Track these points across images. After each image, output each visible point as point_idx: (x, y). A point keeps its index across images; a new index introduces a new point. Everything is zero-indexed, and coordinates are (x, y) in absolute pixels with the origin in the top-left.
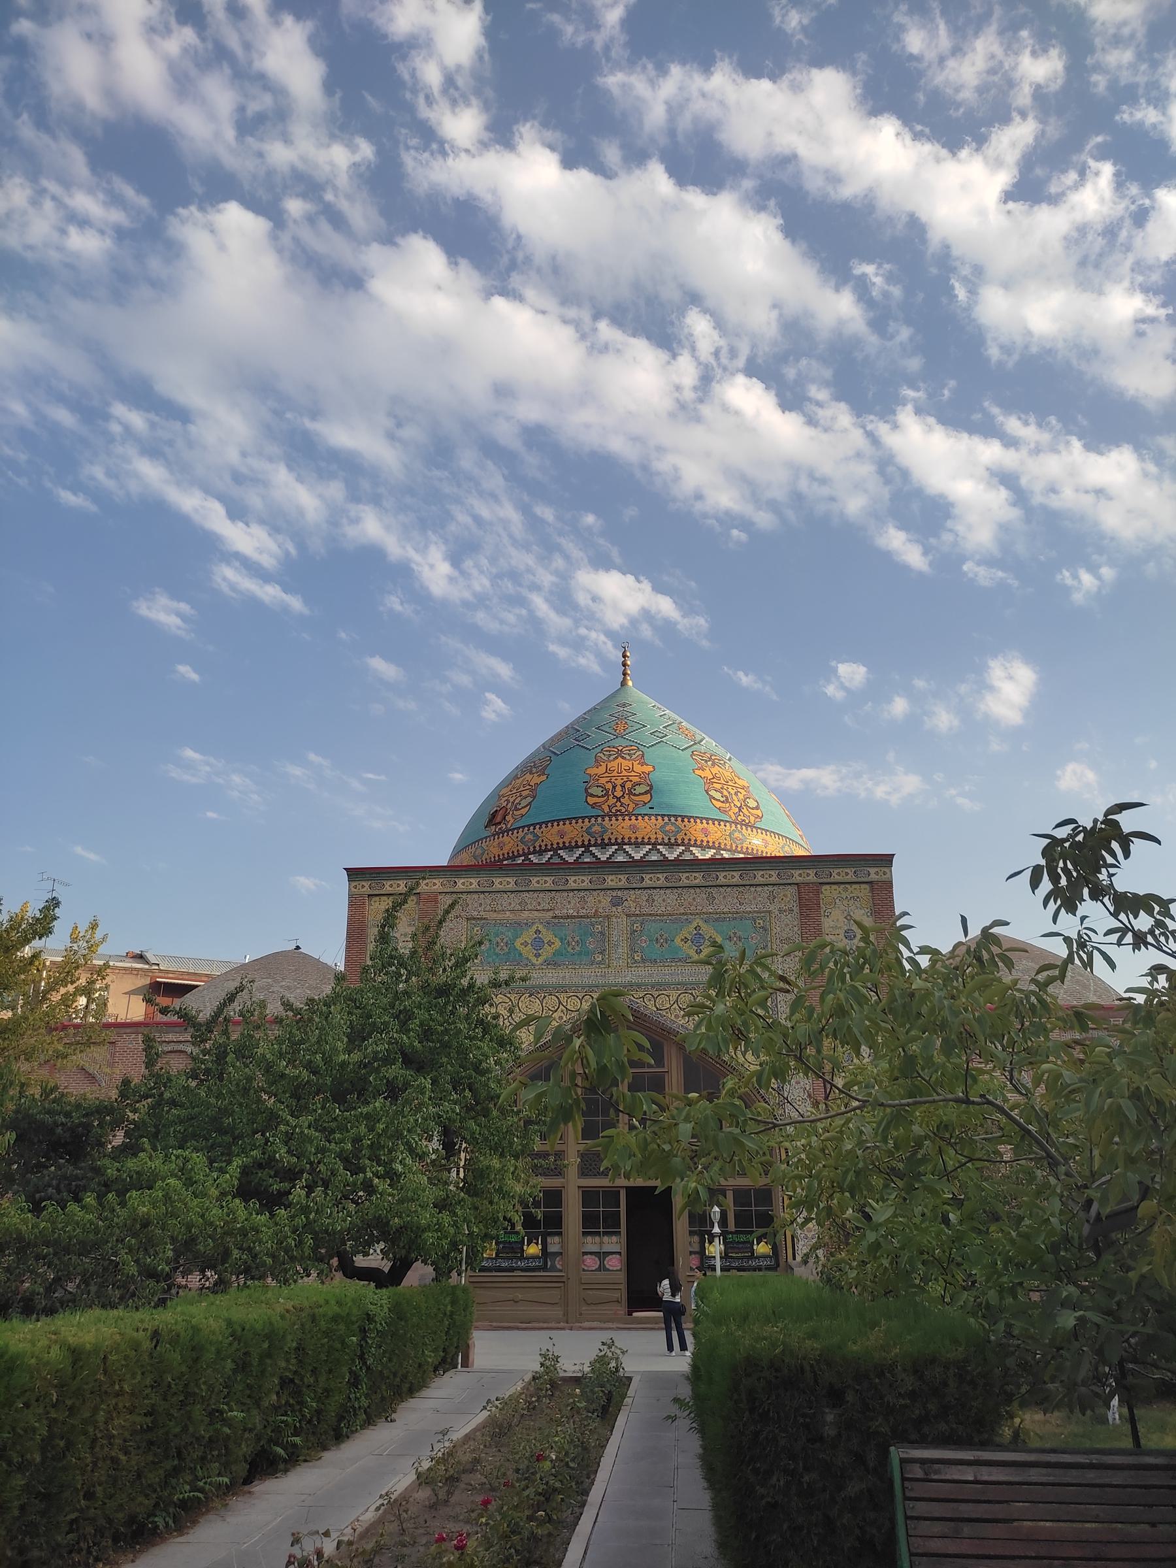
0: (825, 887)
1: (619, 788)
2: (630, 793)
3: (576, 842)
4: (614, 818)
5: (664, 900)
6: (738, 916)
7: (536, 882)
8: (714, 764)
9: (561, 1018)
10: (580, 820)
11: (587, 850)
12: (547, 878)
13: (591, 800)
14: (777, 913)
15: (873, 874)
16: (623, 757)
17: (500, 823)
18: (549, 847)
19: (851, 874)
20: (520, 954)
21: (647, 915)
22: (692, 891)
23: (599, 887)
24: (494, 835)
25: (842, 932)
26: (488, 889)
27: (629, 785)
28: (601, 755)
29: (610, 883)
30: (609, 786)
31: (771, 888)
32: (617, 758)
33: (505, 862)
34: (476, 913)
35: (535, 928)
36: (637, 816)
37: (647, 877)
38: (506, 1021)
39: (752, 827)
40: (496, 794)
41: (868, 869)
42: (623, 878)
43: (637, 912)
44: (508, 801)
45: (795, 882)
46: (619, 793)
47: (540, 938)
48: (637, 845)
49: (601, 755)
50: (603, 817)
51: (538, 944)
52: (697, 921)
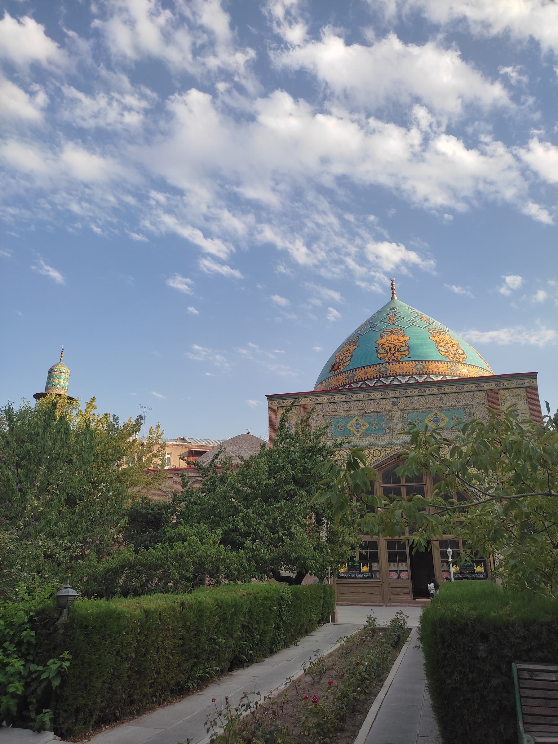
0: (501, 391)
1: (393, 349)
2: (398, 351)
3: (374, 376)
4: (391, 364)
5: (418, 402)
6: (456, 408)
7: (355, 396)
8: (440, 334)
10: (375, 366)
12: (360, 395)
13: (379, 356)
14: (476, 405)
15: (527, 383)
17: (336, 370)
18: (360, 380)
19: (515, 383)
20: (350, 431)
21: (410, 409)
22: (432, 397)
23: (386, 397)
24: (334, 376)
26: (332, 401)
27: (397, 347)
28: (383, 334)
29: (391, 395)
30: (388, 348)
31: (472, 393)
32: (391, 334)
33: (340, 388)
34: (328, 413)
35: (356, 418)
36: (402, 362)
37: (409, 391)
39: (461, 363)
40: (334, 356)
41: (524, 380)
42: (397, 392)
43: (405, 408)
44: (340, 359)
45: (485, 389)
46: (393, 352)
47: (358, 423)
48: (403, 376)
49: (383, 334)
50: (386, 364)
51: (358, 426)
52: (436, 411)
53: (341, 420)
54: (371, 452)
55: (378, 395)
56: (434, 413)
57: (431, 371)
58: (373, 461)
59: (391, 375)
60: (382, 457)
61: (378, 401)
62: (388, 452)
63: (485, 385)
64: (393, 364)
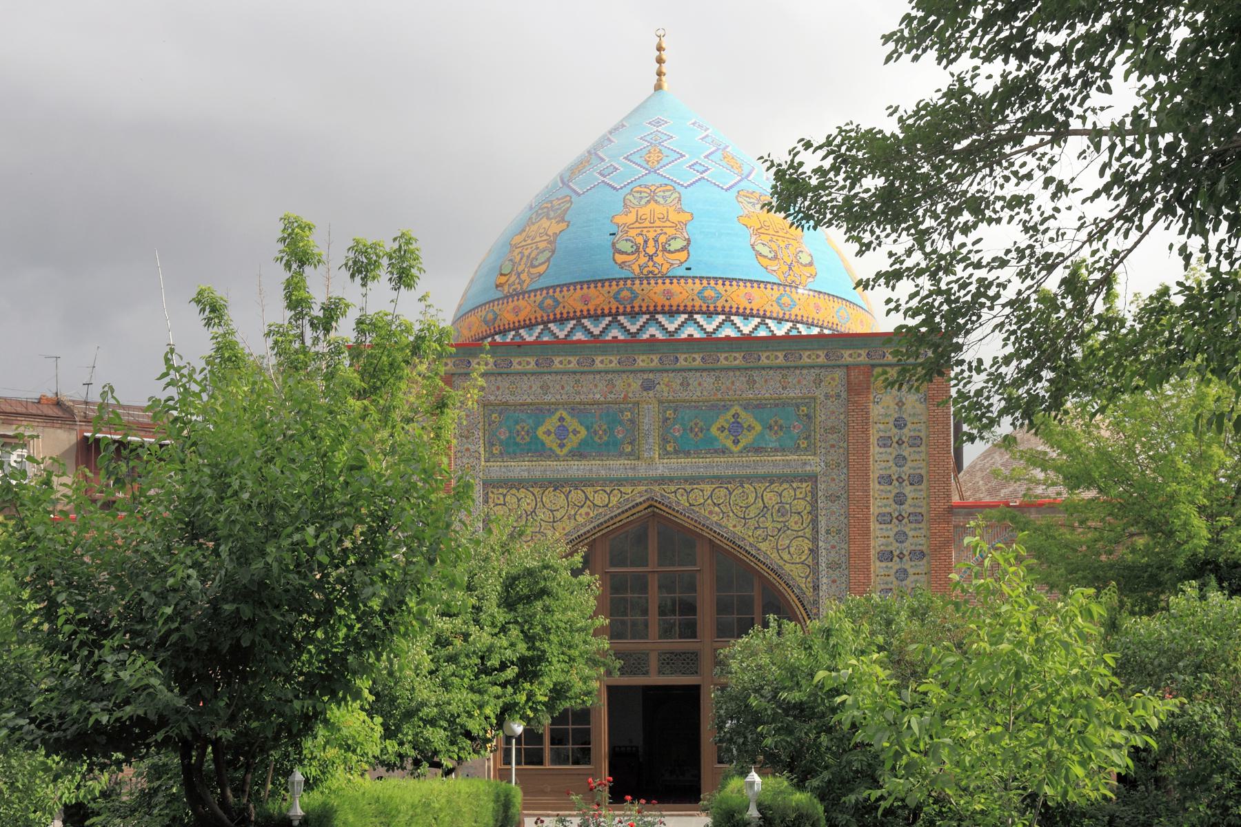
3: (603, 309)
4: (645, 282)
5: (700, 384)
6: (780, 404)
9: (587, 514)
10: (607, 284)
11: (615, 320)
12: (572, 359)
13: (620, 258)
16: (656, 202)
20: (543, 444)
22: (731, 373)
24: (506, 297)
25: (891, 420)
26: (506, 370)
27: (662, 239)
28: (629, 197)
29: (641, 364)
30: (640, 240)
31: (818, 371)
32: (649, 202)
35: (558, 415)
37: (682, 357)
38: (529, 517)
42: (656, 358)
43: (671, 398)
45: (845, 363)
47: (564, 426)
49: (629, 197)
51: (562, 432)
52: (737, 409)
53: (523, 416)
54: (588, 494)
55: (611, 362)
56: (733, 411)
57: (735, 306)
58: (592, 515)
59: (644, 309)
60: (612, 507)
61: (610, 376)
62: (627, 497)
63: (846, 353)
64: (649, 284)
